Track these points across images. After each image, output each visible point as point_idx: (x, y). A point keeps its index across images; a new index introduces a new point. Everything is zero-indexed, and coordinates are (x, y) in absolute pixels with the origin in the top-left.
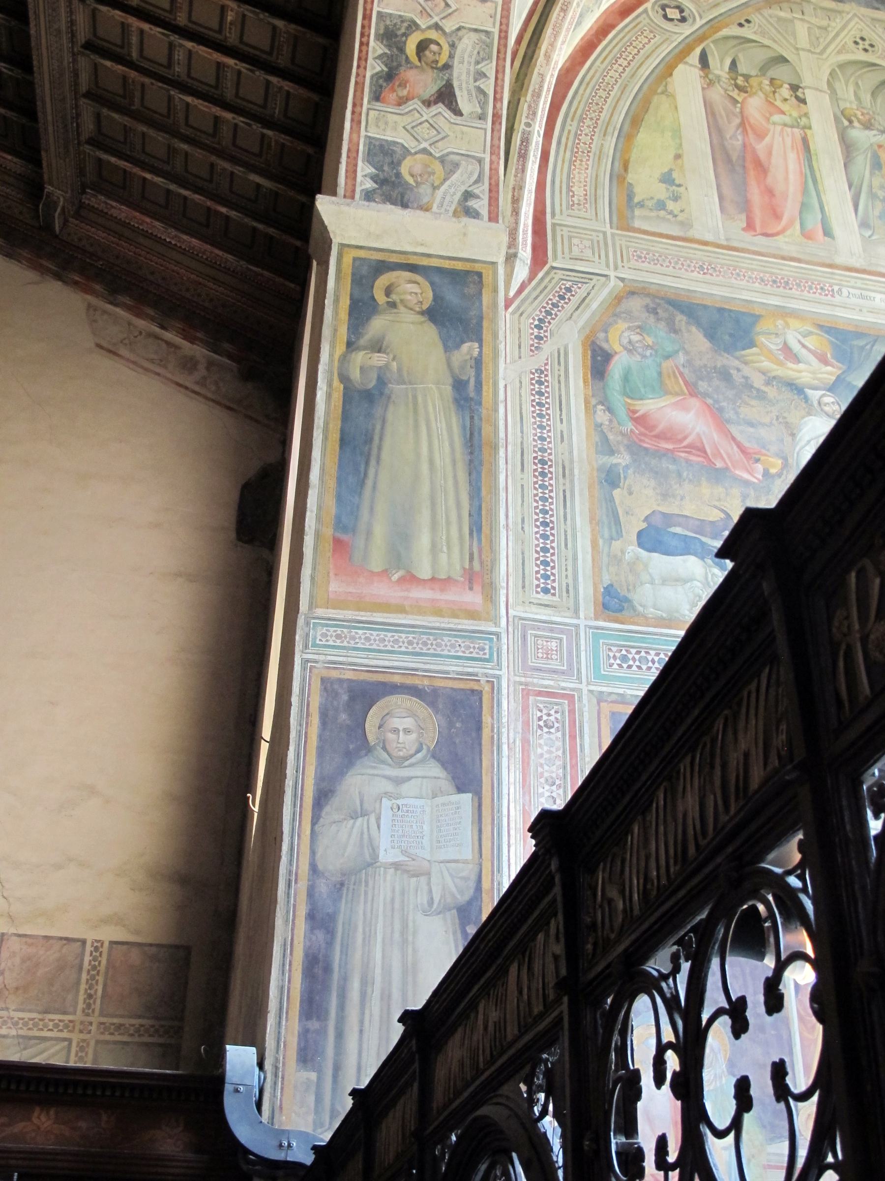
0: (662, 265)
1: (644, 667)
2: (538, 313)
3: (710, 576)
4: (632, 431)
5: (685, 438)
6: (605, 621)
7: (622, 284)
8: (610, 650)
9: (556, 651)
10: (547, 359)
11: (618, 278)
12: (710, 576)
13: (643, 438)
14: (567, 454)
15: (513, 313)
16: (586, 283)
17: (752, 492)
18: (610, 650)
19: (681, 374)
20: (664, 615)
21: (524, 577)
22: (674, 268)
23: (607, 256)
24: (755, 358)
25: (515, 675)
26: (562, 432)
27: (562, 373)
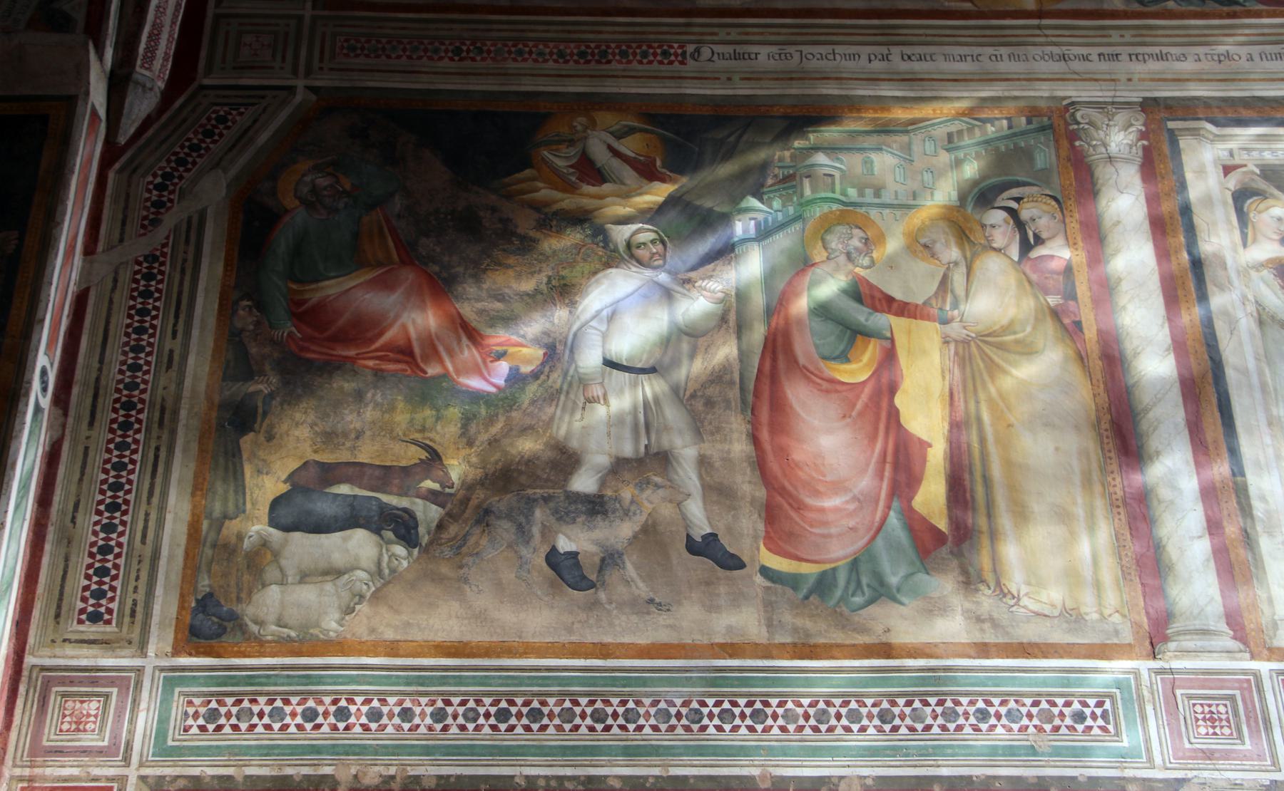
0: (389, 57)
1: (244, 726)
2: (163, 164)
3: (386, 558)
4: (290, 335)
5: (381, 334)
6: (190, 655)
7: (313, 98)
8: (190, 703)
9: (96, 716)
10: (168, 238)
11: (307, 87)
12: (386, 558)
13: (306, 345)
14: (173, 387)
15: (120, 171)
16: (253, 104)
17: (483, 411)
18: (190, 703)
19: (393, 231)
20: (293, 634)
21: (61, 599)
22: (410, 57)
23: (296, 57)
24: (524, 186)
25: (15, 766)
26: (171, 352)
27: (190, 257)
